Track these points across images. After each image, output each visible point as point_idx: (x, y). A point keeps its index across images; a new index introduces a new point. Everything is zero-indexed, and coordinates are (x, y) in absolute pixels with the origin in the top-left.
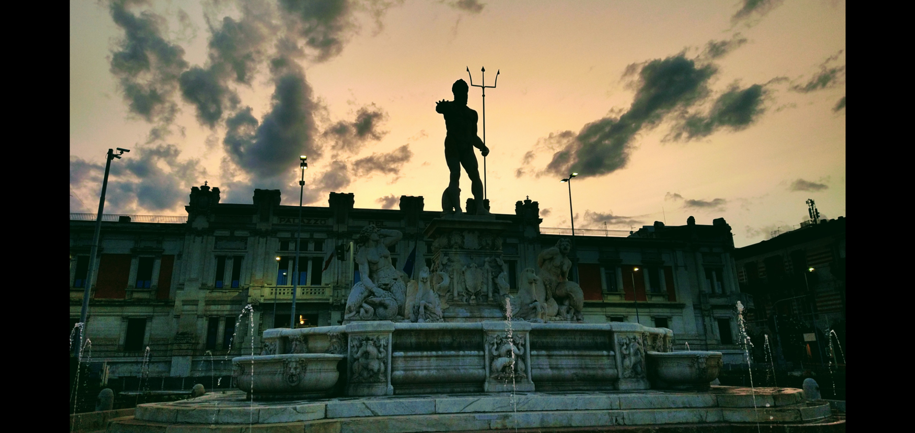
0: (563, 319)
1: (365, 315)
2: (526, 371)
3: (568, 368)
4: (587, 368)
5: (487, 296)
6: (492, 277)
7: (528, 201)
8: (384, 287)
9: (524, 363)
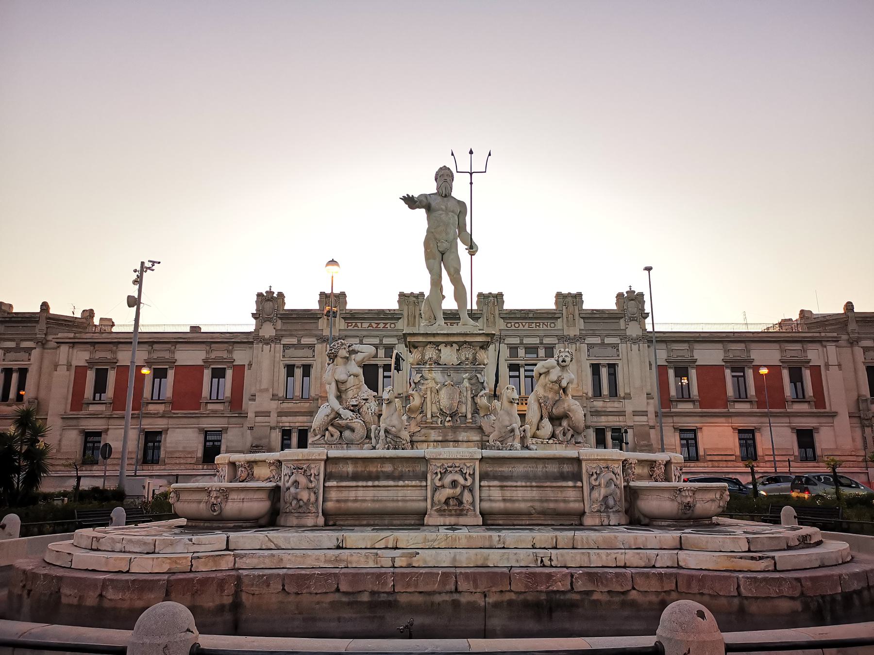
0: (557, 442)
1: (330, 439)
2: (473, 503)
3: (524, 501)
4: (547, 501)
5: (466, 416)
6: (472, 395)
7: (631, 292)
8: (352, 408)
9: (472, 495)
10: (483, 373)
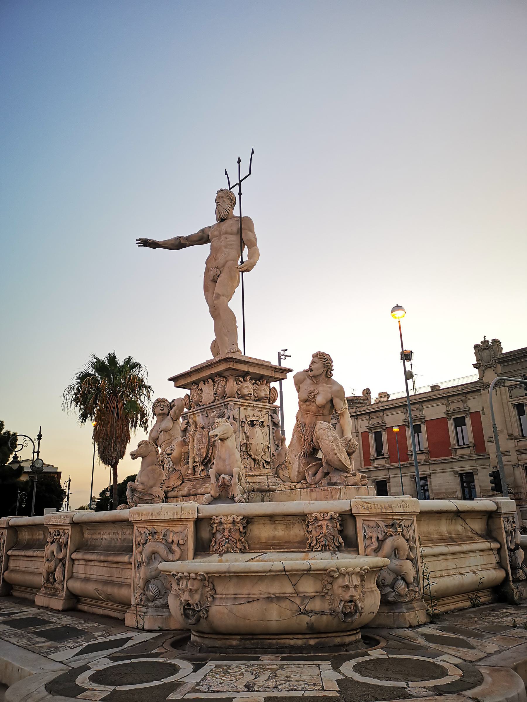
10: (229, 408)
